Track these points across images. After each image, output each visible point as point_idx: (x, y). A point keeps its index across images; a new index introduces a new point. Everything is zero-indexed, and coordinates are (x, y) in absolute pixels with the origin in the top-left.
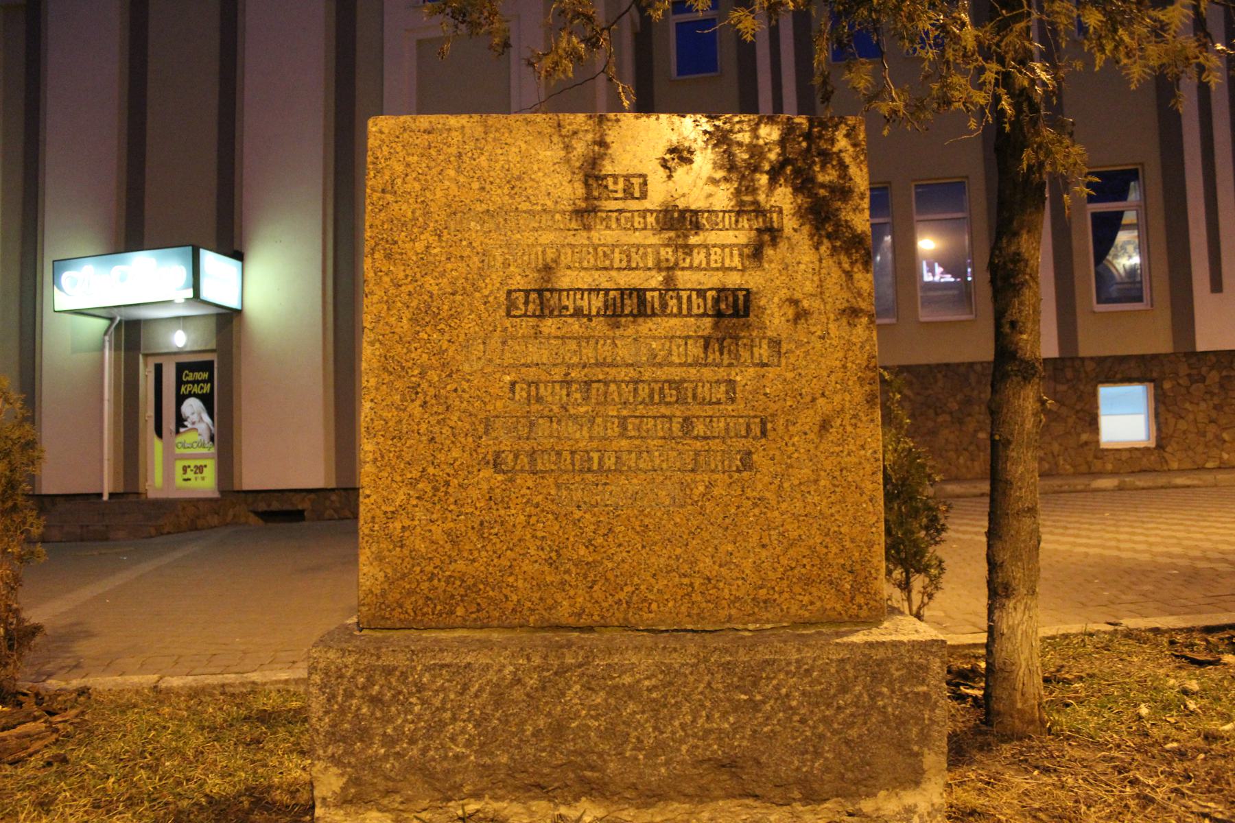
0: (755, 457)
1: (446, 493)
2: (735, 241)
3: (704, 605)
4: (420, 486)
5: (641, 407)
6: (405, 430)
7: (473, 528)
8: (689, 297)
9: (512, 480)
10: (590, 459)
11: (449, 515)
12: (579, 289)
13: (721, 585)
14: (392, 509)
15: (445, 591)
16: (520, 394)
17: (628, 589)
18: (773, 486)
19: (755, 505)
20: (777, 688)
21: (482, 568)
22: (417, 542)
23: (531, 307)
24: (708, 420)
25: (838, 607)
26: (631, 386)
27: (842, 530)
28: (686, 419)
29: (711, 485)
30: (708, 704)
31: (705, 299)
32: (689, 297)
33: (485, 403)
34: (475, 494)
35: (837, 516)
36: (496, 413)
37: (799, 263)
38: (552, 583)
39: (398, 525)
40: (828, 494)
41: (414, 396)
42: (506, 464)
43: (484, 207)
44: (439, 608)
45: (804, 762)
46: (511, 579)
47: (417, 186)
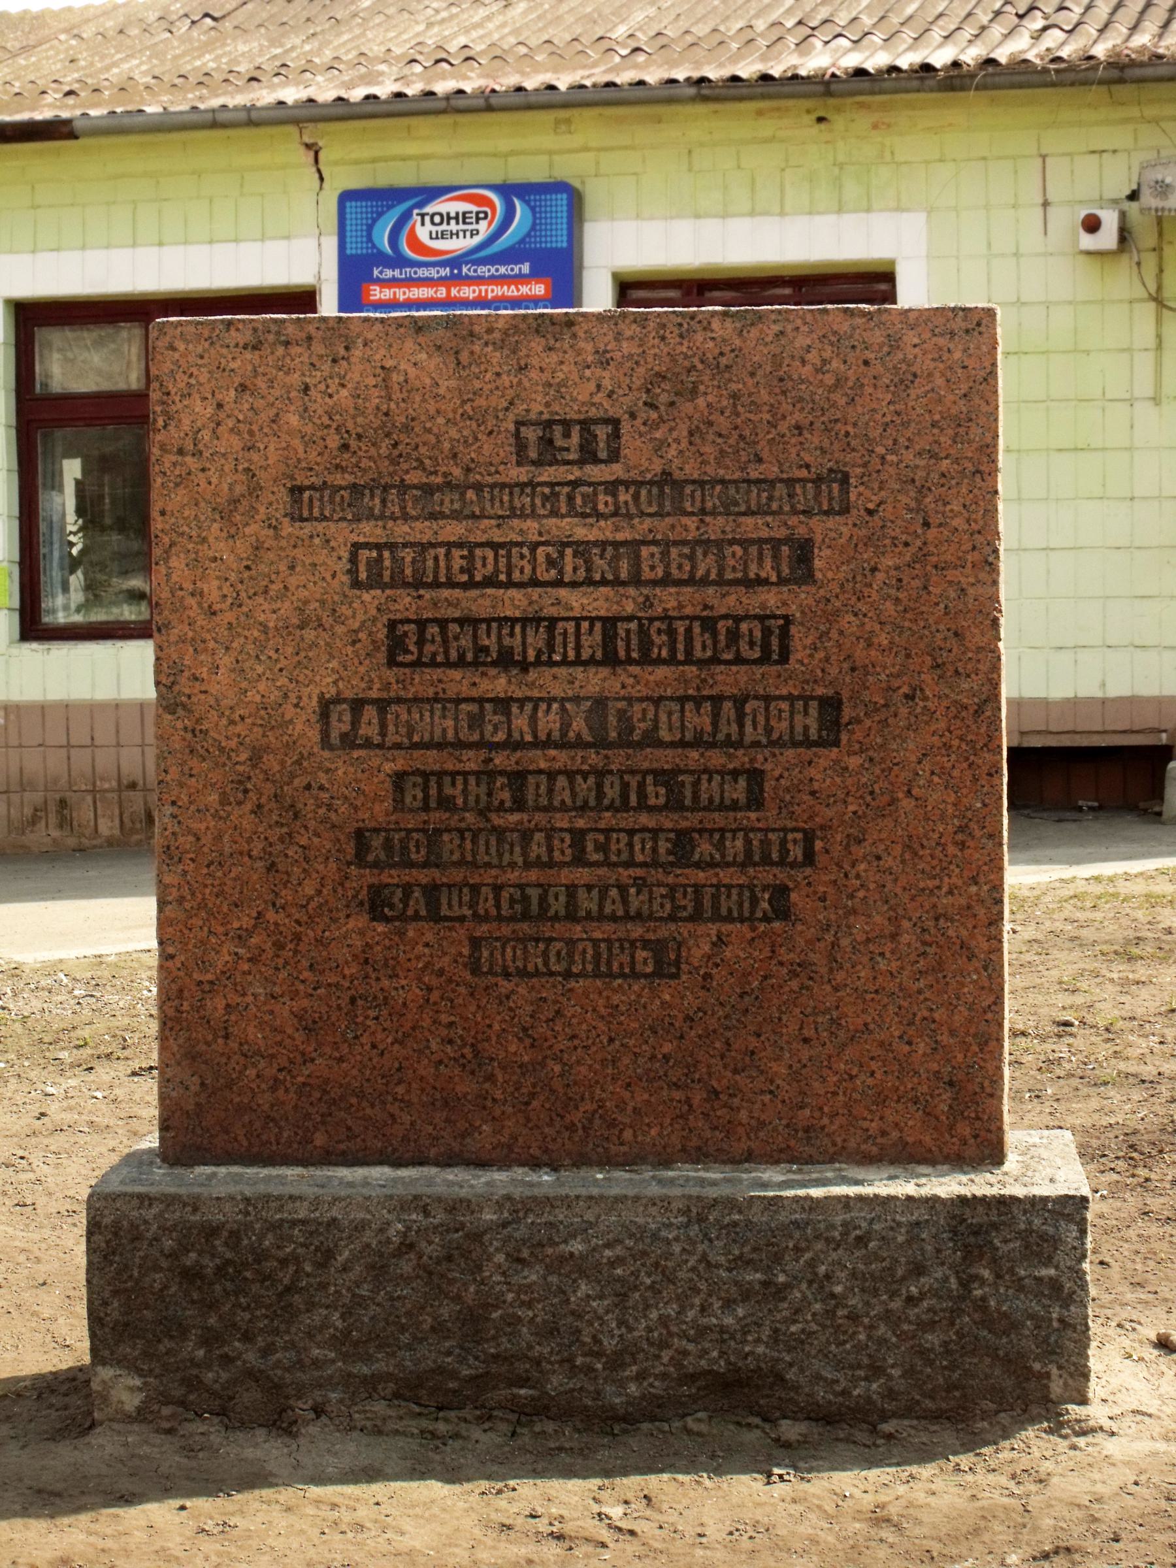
0: (794, 896)
1: (296, 952)
2: (765, 533)
3: (708, 1134)
4: (253, 940)
5: (608, 814)
6: (227, 850)
7: (339, 1008)
8: (689, 630)
9: (402, 934)
10: (526, 899)
11: (301, 987)
12: (506, 619)
13: (736, 1101)
14: (209, 977)
15: (296, 1107)
16: (413, 794)
17: (588, 1106)
18: (822, 944)
19: (794, 974)
20: (812, 1264)
21: (355, 1072)
22: (251, 1030)
23: (429, 648)
24: (717, 836)
25: (927, 1139)
26: (591, 780)
27: (936, 1016)
28: (680, 833)
29: (720, 941)
30: (703, 1286)
31: (715, 634)
32: (689, 630)
33: (356, 809)
34: (342, 954)
35: (928, 994)
36: (373, 824)
37: (874, 570)
38: (465, 1095)
39: (220, 1003)
40: (913, 957)
41: (240, 795)
42: (392, 907)
43: (350, 478)
44: (285, 1135)
45: (855, 1380)
46: (400, 1090)
47: (236, 442)
